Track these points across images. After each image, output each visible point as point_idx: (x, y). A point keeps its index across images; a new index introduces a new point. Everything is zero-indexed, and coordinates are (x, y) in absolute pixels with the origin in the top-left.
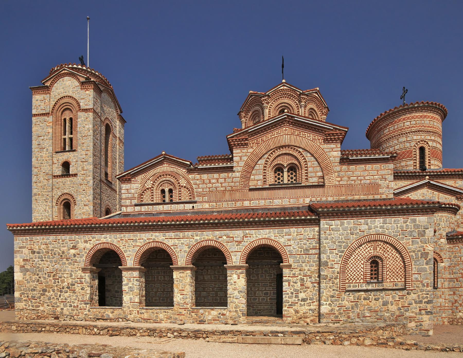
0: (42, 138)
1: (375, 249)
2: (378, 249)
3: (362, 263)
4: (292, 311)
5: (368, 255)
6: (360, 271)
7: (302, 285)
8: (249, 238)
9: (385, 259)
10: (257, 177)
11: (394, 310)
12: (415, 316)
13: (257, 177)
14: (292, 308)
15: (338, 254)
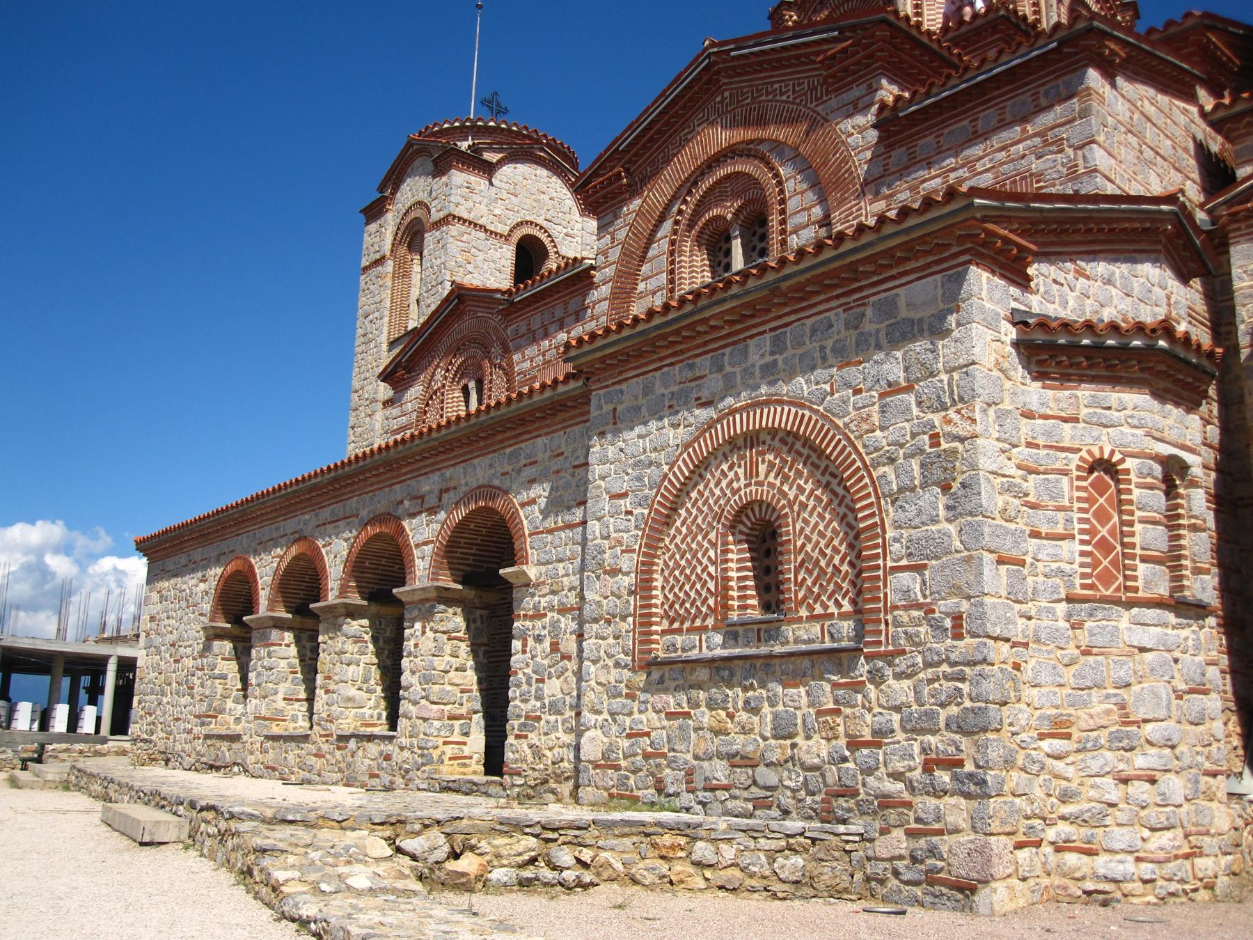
0: (371, 317)
1: (752, 473)
2: (762, 469)
3: (710, 541)
4: (526, 748)
5: (729, 500)
6: (705, 576)
7: (555, 647)
8: (452, 493)
9: (787, 510)
10: (653, 284)
11: (816, 761)
12: (906, 796)
13: (653, 284)
14: (526, 737)
15: (630, 513)
